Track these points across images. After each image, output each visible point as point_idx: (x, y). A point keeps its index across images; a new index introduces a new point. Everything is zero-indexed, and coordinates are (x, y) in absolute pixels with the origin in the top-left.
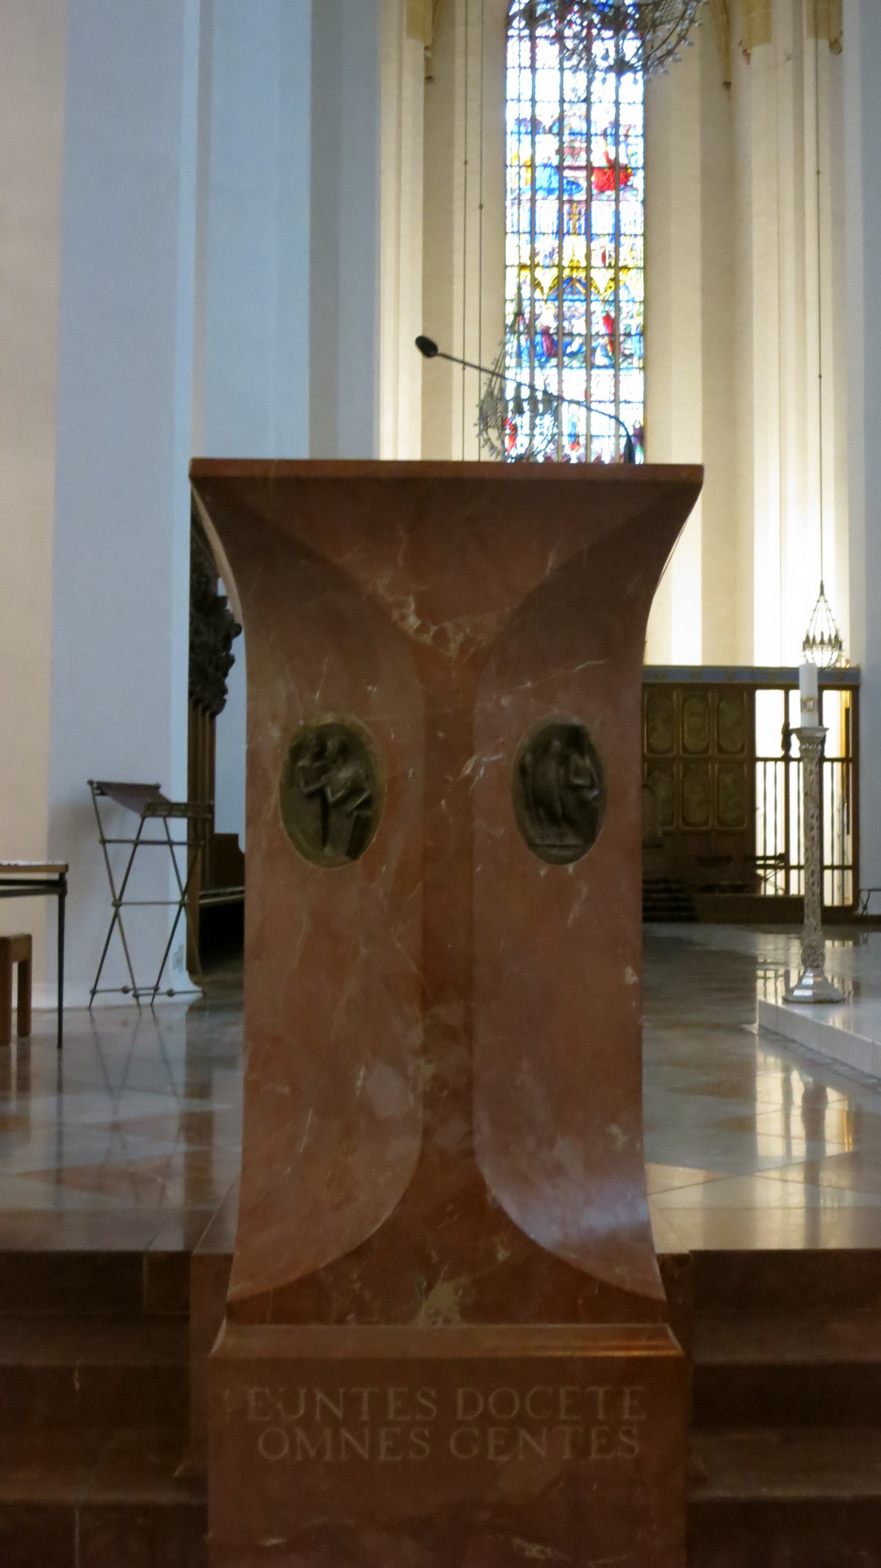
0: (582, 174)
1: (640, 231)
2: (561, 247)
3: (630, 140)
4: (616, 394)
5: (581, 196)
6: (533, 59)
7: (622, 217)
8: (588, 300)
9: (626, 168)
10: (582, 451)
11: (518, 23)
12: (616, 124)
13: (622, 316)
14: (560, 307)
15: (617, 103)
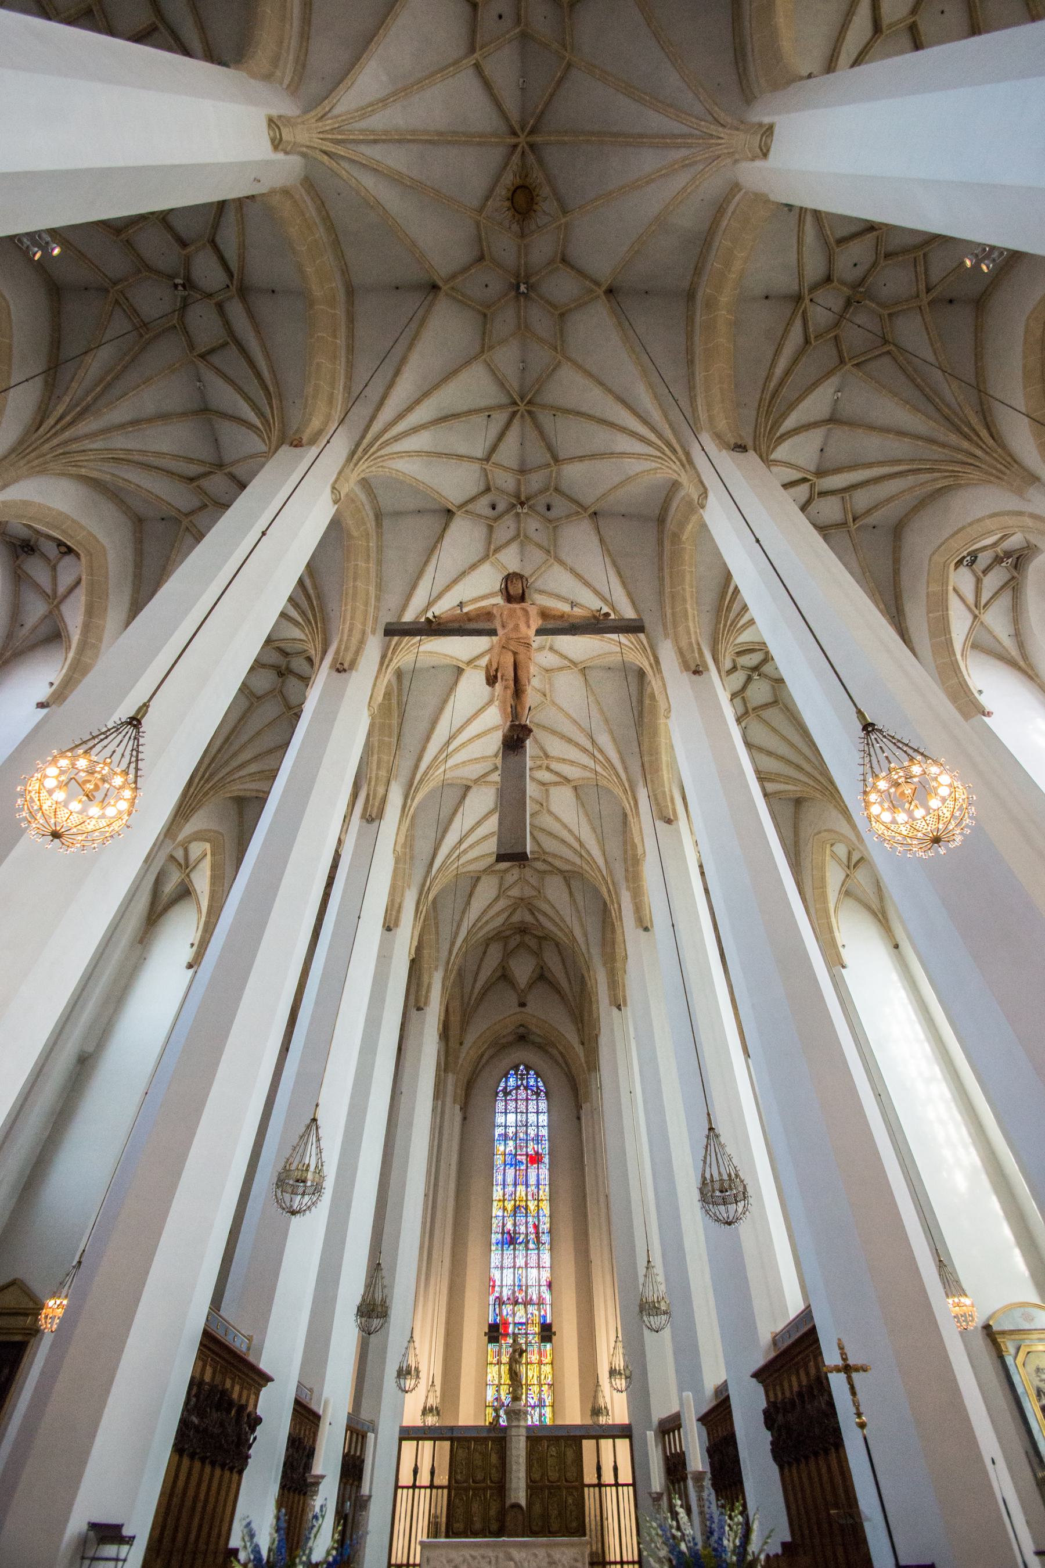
0: (524, 1157)
1: (547, 1183)
2: (515, 1191)
4: (539, 1264)
5: (523, 1167)
6: (506, 1109)
8: (526, 1216)
10: (524, 1294)
11: (501, 1094)
12: (537, 1135)
14: (515, 1220)
15: (538, 1126)
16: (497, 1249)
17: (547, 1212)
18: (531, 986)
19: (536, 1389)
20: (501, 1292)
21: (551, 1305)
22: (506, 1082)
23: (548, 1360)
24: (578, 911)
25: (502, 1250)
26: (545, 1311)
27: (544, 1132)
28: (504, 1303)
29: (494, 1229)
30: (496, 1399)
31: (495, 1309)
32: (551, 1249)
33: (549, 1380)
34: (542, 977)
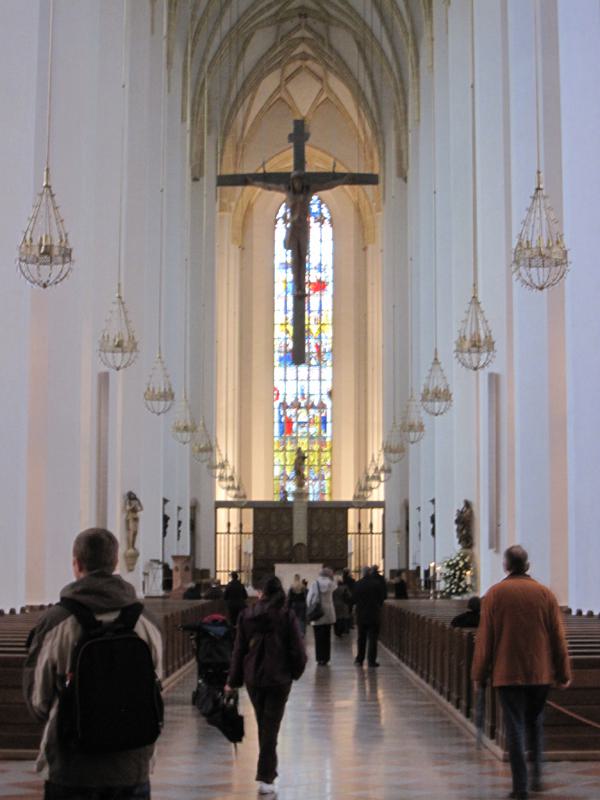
12: (320, 264)
13: (323, 344)
16: (280, 365)
18: (316, 107)
19: (317, 468)
21: (332, 408)
23: (328, 448)
27: (328, 262)
28: (288, 407)
29: (276, 348)
32: (332, 365)
33: (328, 463)
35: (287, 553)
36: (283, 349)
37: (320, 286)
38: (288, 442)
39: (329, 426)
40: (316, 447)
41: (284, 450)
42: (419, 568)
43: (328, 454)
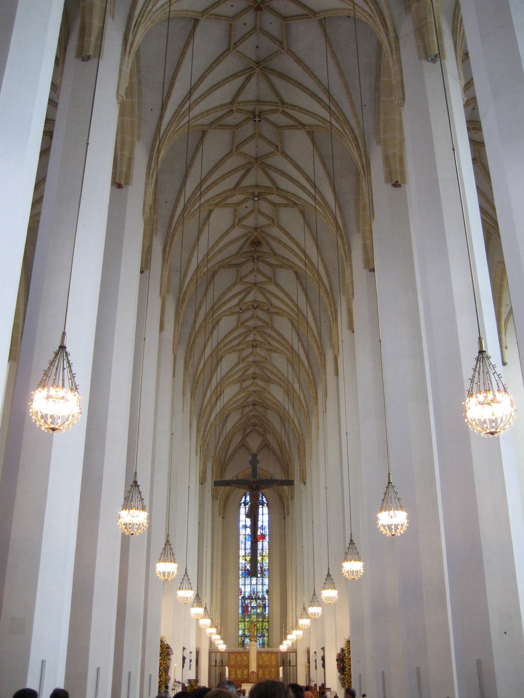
1: (267, 548)
3: (266, 529)
4: (262, 583)
7: (264, 545)
9: (264, 535)
11: (243, 505)
12: (262, 526)
15: (263, 522)
16: (242, 577)
17: (267, 562)
18: (260, 449)
20: (245, 595)
21: (268, 600)
22: (245, 498)
24: (285, 427)
25: (245, 578)
26: (266, 602)
27: (266, 524)
28: (246, 599)
30: (243, 634)
31: (242, 601)
34: (266, 445)
35: (246, 677)
36: (243, 569)
37: (263, 537)
38: (246, 617)
39: (267, 608)
40: (260, 620)
41: (244, 621)
42: (316, 685)
43: (266, 623)
